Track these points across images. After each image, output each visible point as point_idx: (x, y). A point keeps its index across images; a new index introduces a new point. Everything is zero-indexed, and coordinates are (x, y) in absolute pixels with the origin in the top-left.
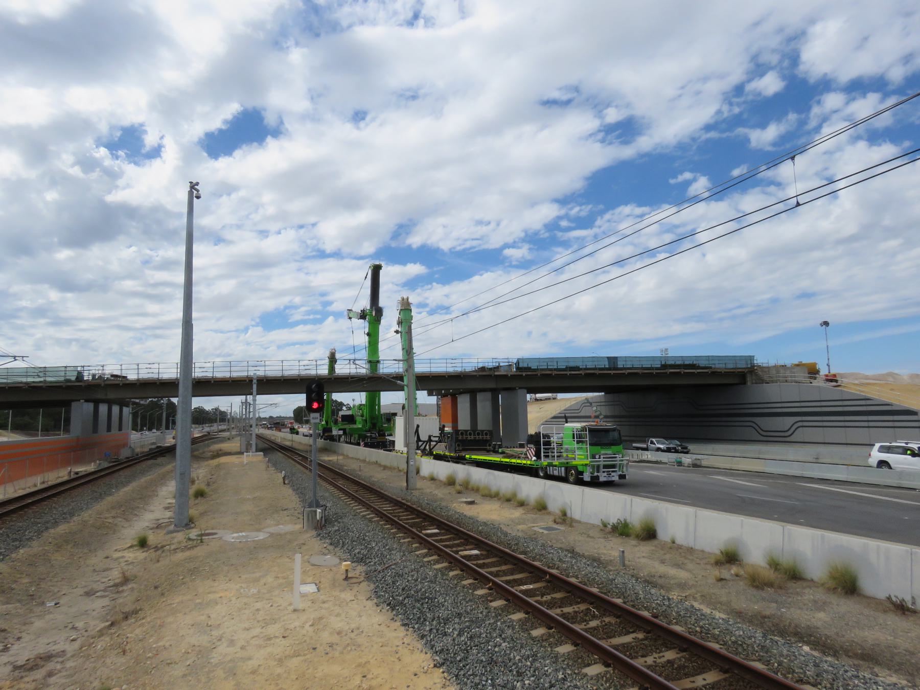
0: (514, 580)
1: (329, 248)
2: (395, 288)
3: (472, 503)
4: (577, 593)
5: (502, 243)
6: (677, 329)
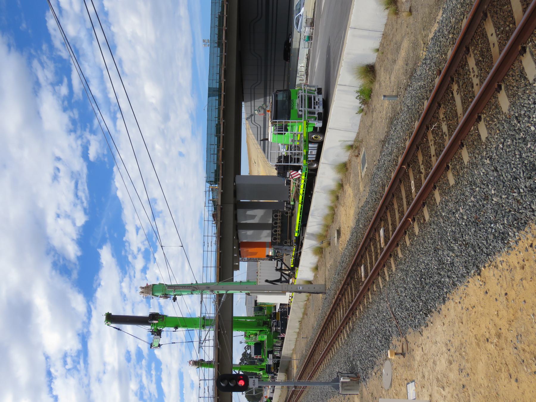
0: (407, 197)
1: (73, 345)
2: (127, 279)
3: (339, 232)
4: (418, 142)
5: (82, 160)
6: (183, 11)
